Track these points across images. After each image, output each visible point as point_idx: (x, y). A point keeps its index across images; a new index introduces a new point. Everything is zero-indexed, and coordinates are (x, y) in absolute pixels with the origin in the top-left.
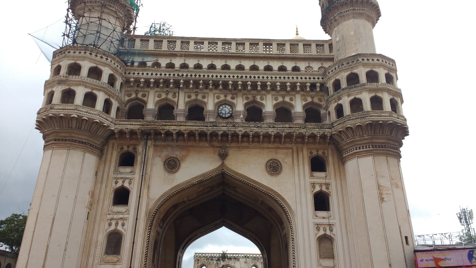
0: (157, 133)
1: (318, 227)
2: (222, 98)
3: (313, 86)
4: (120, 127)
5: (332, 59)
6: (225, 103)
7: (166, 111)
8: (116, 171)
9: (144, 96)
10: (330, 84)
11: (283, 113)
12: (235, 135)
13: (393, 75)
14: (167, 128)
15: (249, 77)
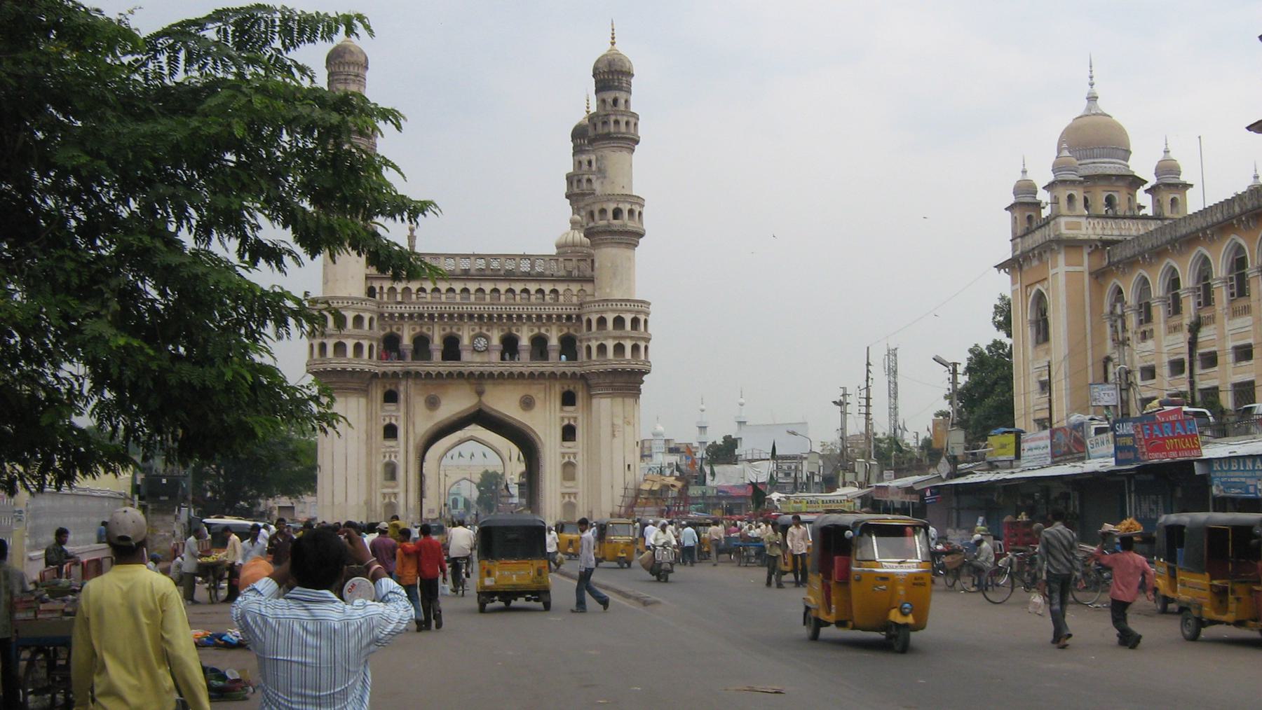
0: (418, 374)
1: (563, 455)
2: (477, 330)
3: (569, 318)
4: (383, 369)
5: (591, 280)
6: (481, 335)
7: (421, 343)
8: (382, 407)
9: (398, 329)
10: (584, 319)
11: (539, 343)
12: (491, 375)
13: (642, 318)
14: (427, 369)
15: (504, 306)
